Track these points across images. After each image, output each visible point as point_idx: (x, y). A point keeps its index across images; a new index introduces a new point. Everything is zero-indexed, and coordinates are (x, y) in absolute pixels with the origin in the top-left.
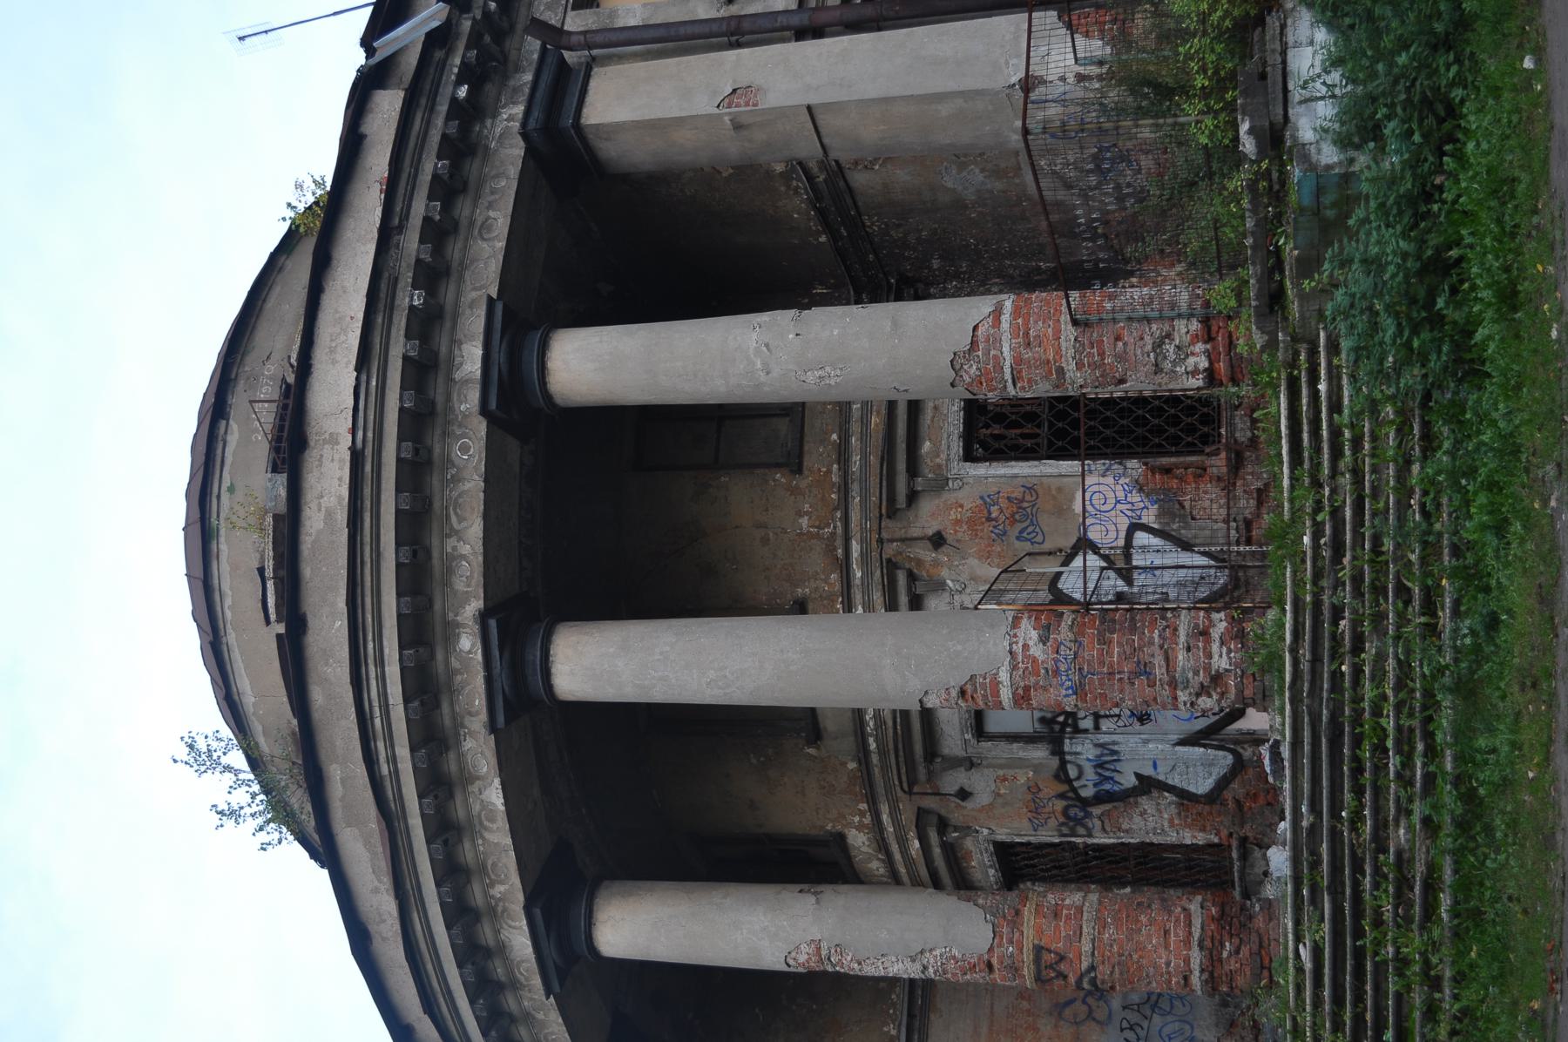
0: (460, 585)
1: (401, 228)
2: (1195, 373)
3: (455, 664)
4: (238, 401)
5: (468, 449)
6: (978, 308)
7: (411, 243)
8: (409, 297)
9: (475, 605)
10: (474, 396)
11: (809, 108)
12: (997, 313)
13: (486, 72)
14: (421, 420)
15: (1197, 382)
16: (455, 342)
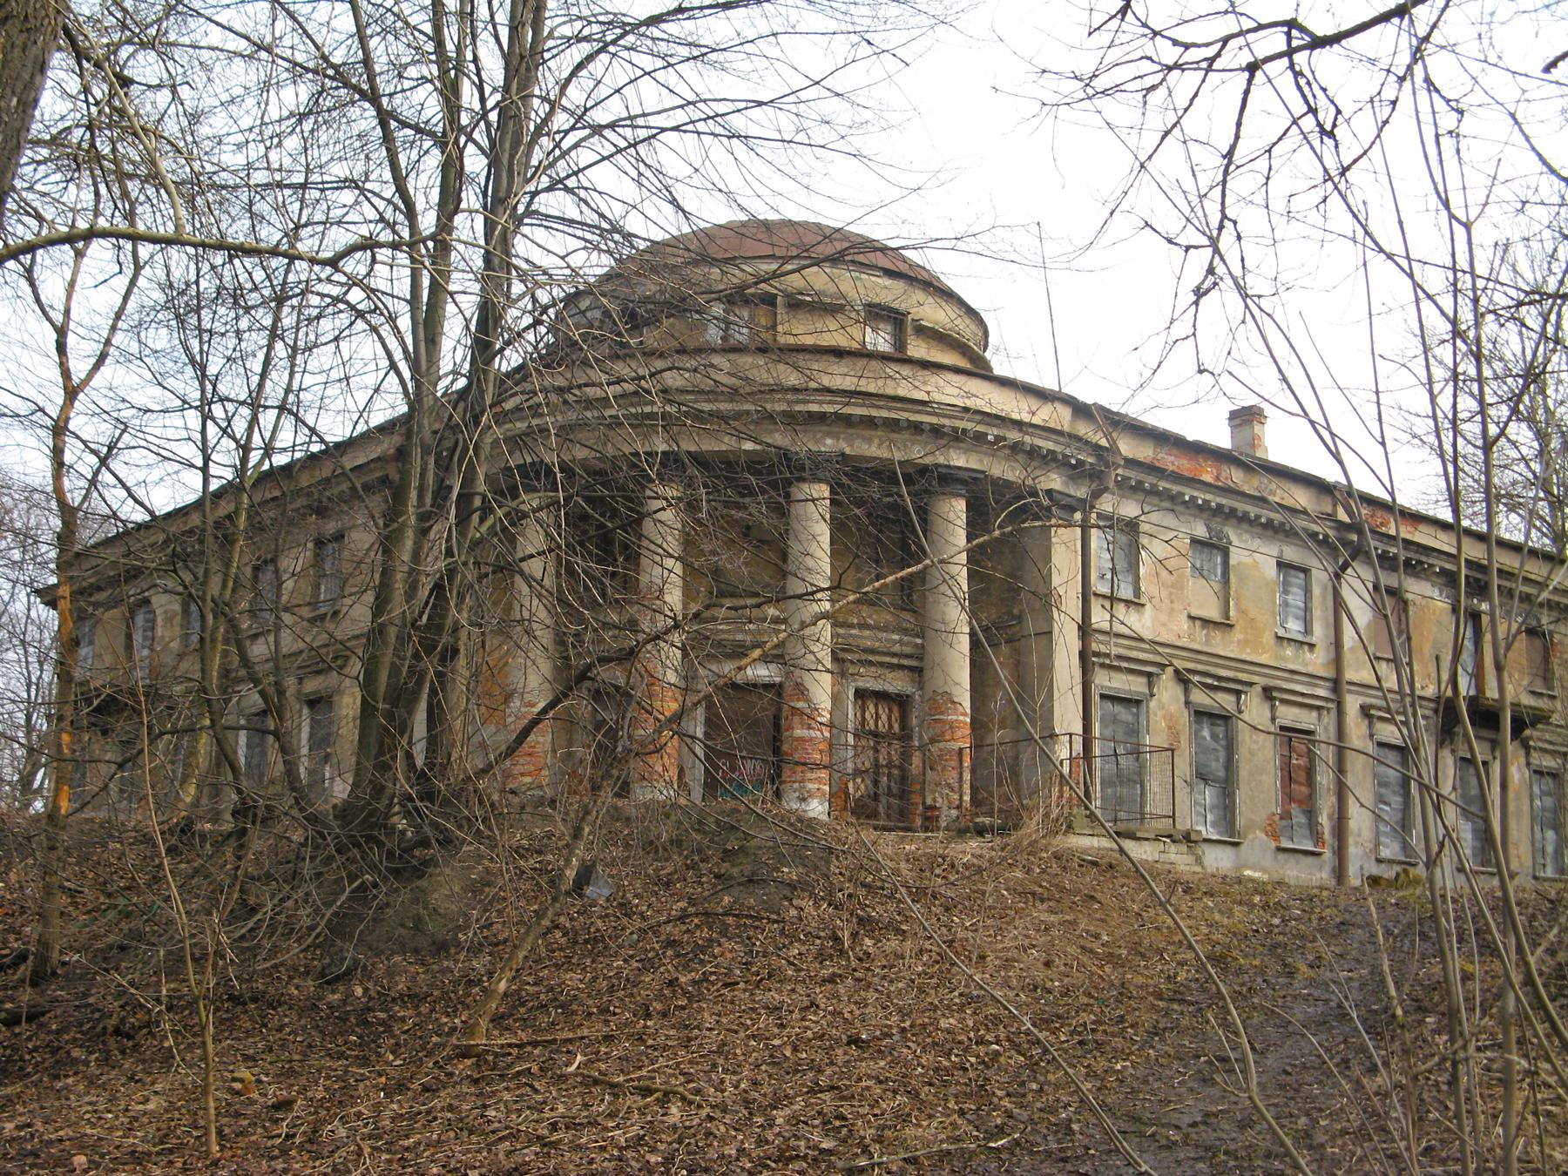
0: (858, 443)
1: (1020, 430)
2: (934, 800)
3: (819, 435)
4: (898, 286)
5: (918, 452)
6: (967, 704)
7: (1014, 435)
8: (992, 433)
9: (848, 451)
10: (941, 460)
11: (1050, 633)
12: (965, 714)
13: (1076, 471)
14: (936, 431)
15: (929, 801)
16: (966, 451)
